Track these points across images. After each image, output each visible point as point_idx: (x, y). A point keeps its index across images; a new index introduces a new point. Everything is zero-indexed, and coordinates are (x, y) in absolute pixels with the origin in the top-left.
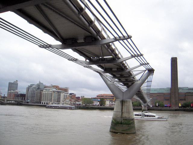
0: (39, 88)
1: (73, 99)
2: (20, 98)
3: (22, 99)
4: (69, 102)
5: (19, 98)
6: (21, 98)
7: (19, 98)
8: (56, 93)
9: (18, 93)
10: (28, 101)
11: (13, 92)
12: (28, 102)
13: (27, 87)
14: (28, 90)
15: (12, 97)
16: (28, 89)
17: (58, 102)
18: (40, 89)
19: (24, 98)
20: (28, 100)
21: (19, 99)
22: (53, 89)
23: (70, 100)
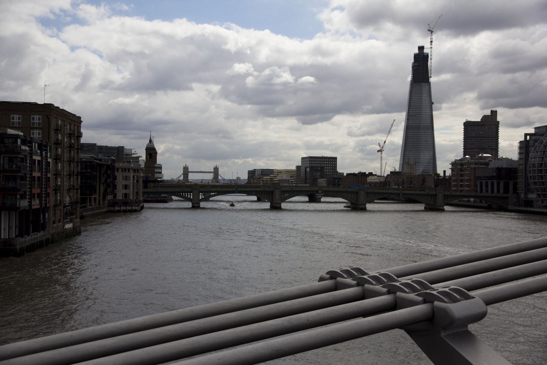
2: (498, 184)
3: (506, 190)
5: (492, 184)
7: (492, 184)
9: (487, 164)
10: (532, 196)
12: (529, 203)
13: (522, 139)
15: (468, 180)
16: (525, 146)
19: (515, 184)
20: (528, 191)
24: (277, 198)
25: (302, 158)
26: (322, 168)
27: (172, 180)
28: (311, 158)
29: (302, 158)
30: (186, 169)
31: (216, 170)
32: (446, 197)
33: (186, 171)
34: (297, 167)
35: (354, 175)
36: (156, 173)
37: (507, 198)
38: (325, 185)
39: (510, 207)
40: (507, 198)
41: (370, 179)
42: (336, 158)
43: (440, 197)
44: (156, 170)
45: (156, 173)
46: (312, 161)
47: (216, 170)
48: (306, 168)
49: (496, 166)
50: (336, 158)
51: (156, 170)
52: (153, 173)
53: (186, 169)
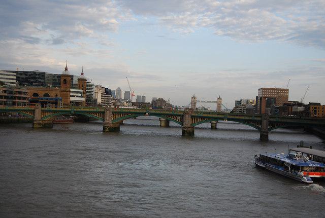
24: (108, 118)
27: (176, 108)
30: (194, 97)
31: (219, 99)
33: (194, 102)
34: (257, 97)
36: (71, 96)
44: (72, 94)
45: (71, 96)
46: (264, 92)
47: (219, 99)
48: (261, 98)
50: (288, 90)
51: (72, 94)
52: (67, 97)
53: (194, 97)
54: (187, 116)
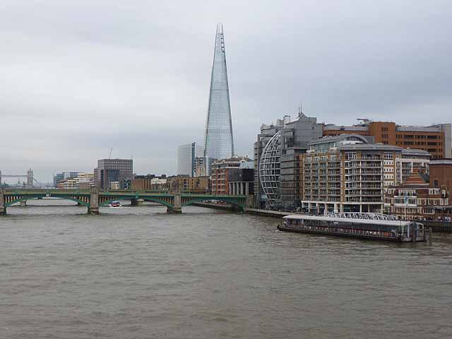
0: (292, 142)
1: (436, 185)
4: (412, 202)
6: (247, 187)
8: (355, 158)
9: (238, 165)
10: (264, 197)
11: (225, 165)
12: (262, 204)
14: (260, 154)
15: (223, 182)
16: (259, 148)
17: (369, 199)
18: (299, 144)
20: (262, 193)
21: (239, 190)
22: (345, 142)
23: (422, 193)
25: (99, 161)
26: (118, 170)
28: (105, 160)
29: (99, 161)
31: (30, 172)
32: (183, 199)
34: (96, 170)
35: (142, 177)
37: (245, 199)
38: (117, 188)
39: (245, 209)
40: (245, 199)
41: (154, 181)
42: (131, 161)
43: (177, 199)
47: (30, 172)
48: (102, 171)
49: (244, 167)
50: (131, 161)
54: (95, 195)
